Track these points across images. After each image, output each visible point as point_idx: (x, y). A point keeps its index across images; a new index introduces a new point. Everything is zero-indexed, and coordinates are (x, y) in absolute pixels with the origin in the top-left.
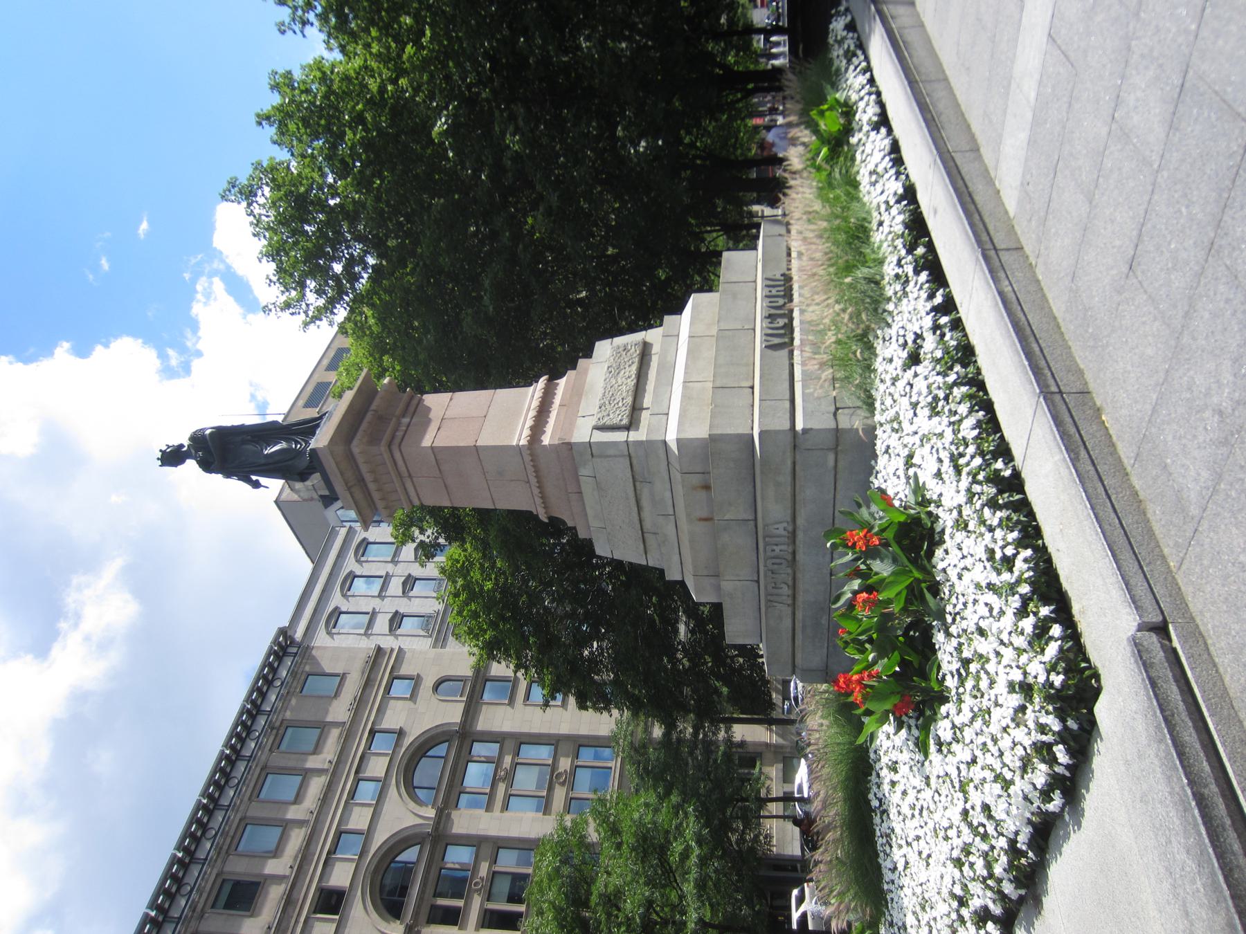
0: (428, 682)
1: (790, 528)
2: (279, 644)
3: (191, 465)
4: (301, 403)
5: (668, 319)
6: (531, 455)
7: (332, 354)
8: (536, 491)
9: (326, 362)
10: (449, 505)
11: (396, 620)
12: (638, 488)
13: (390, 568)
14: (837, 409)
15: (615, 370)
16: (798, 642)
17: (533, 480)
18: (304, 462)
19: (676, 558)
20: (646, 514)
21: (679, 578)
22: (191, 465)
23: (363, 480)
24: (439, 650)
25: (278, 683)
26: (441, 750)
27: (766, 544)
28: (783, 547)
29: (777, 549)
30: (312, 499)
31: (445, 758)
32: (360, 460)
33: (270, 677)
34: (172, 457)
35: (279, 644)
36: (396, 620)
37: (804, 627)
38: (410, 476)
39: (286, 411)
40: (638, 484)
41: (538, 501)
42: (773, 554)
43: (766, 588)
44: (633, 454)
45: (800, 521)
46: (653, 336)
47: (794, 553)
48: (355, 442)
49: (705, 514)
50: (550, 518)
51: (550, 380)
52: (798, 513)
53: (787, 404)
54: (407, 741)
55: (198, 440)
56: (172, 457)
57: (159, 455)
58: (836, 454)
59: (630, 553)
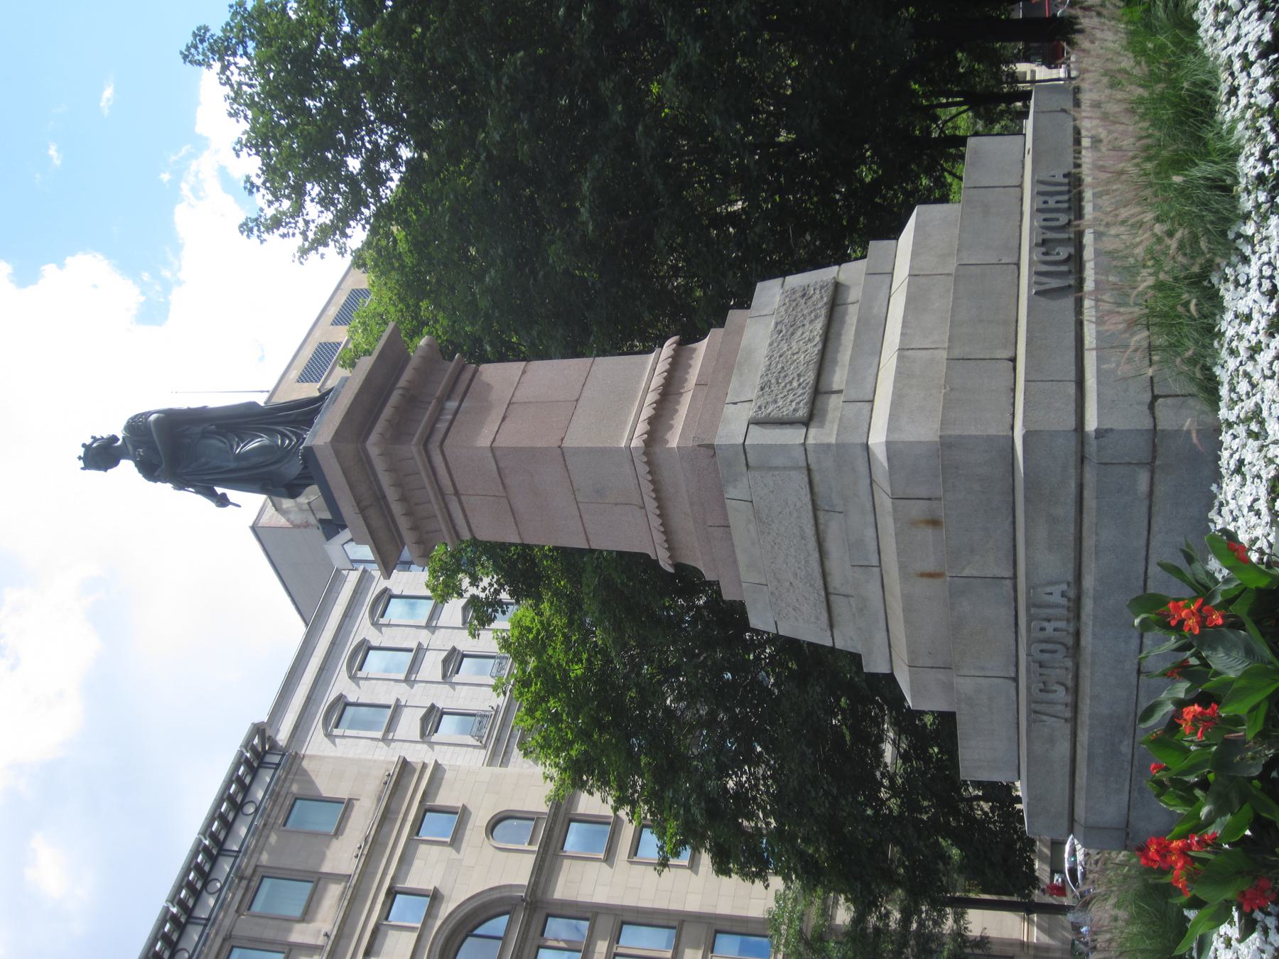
0: (480, 819)
1: (1072, 594)
2: (253, 749)
3: (127, 467)
4: (294, 374)
5: (876, 247)
6: (649, 463)
7: (342, 298)
8: (656, 522)
9: (333, 311)
10: (518, 541)
11: (432, 718)
12: (822, 520)
13: (424, 637)
14: (1155, 398)
15: (787, 329)
16: (1081, 780)
17: (651, 505)
18: (293, 468)
19: (880, 637)
20: (834, 565)
23: (384, 497)
24: (497, 770)
25: (250, 809)
26: (498, 925)
27: (1030, 618)
28: (1062, 624)
29: (1049, 627)
30: (307, 525)
31: (503, 939)
32: (380, 465)
33: (239, 799)
34: (101, 455)
35: (253, 749)
36: (432, 718)
38: (457, 493)
39: (271, 387)
40: (821, 514)
41: (659, 538)
42: (1041, 635)
43: (1029, 688)
44: (813, 466)
45: (1089, 582)
46: (851, 273)
47: (1077, 634)
48: (374, 437)
49: (931, 567)
50: (677, 566)
51: (680, 344)
52: (1085, 570)
53: (1071, 389)
54: (446, 910)
55: (137, 427)
56: (101, 455)
57: (81, 452)
58: (1152, 472)
59: (810, 630)
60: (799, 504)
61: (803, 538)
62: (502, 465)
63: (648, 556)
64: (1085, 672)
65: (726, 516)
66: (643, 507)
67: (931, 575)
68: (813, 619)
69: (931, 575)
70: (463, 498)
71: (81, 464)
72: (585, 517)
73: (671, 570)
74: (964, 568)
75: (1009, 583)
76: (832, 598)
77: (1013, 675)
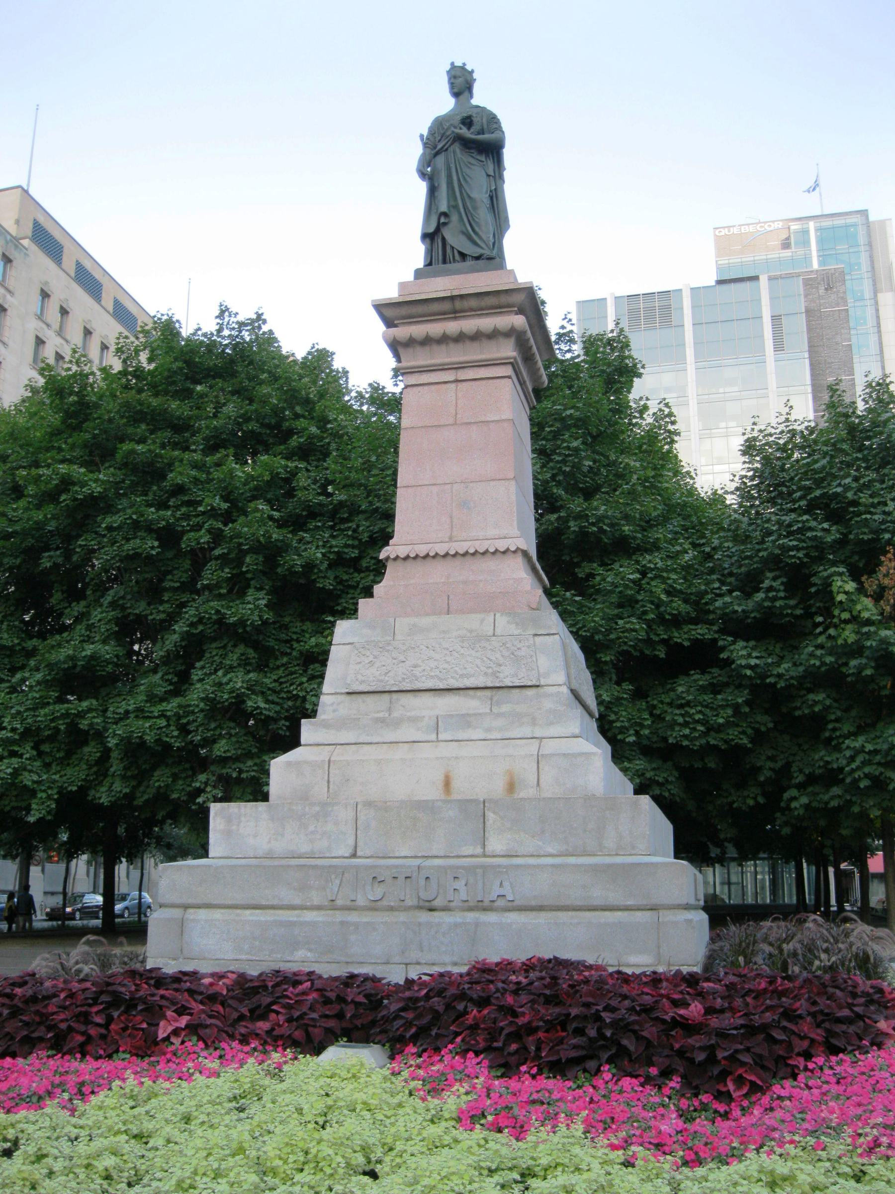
1: (500, 903)
3: (445, 104)
9: (88, 265)
10: (404, 423)
17: (462, 548)
21: (303, 741)
22: (445, 104)
23: (455, 318)
34: (461, 83)
37: (291, 924)
38: (457, 381)
39: (31, 192)
40: (488, 693)
44: (541, 690)
45: (513, 917)
47: (445, 909)
49: (456, 784)
56: (461, 83)
60: (501, 675)
61: (462, 676)
62: (492, 426)
63: (386, 537)
64: (402, 917)
65: (462, 612)
66: (451, 539)
67: (447, 783)
68: (360, 678)
69: (447, 783)
70: (453, 386)
71: (458, 63)
72: (435, 489)
73: (382, 556)
74: (494, 813)
75: (479, 850)
76: (386, 697)
77: (359, 853)
